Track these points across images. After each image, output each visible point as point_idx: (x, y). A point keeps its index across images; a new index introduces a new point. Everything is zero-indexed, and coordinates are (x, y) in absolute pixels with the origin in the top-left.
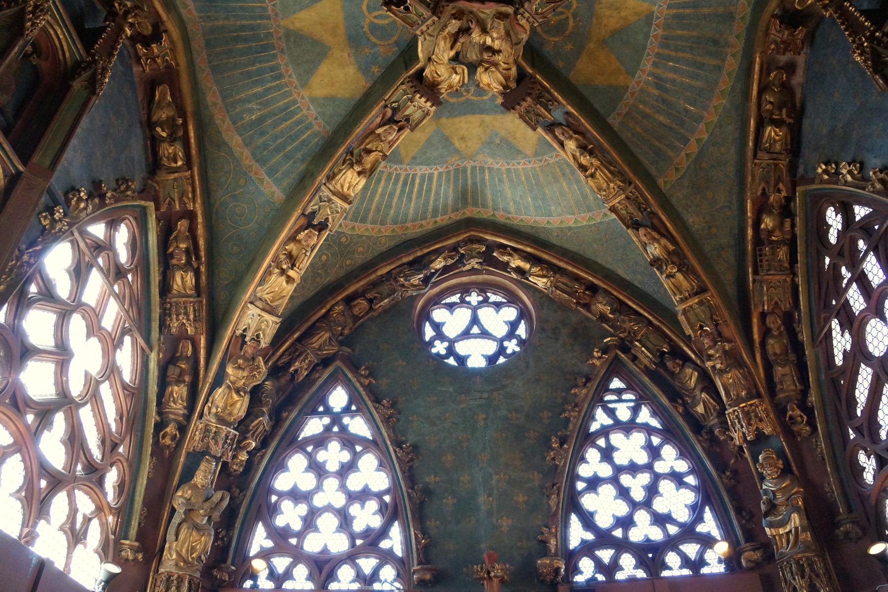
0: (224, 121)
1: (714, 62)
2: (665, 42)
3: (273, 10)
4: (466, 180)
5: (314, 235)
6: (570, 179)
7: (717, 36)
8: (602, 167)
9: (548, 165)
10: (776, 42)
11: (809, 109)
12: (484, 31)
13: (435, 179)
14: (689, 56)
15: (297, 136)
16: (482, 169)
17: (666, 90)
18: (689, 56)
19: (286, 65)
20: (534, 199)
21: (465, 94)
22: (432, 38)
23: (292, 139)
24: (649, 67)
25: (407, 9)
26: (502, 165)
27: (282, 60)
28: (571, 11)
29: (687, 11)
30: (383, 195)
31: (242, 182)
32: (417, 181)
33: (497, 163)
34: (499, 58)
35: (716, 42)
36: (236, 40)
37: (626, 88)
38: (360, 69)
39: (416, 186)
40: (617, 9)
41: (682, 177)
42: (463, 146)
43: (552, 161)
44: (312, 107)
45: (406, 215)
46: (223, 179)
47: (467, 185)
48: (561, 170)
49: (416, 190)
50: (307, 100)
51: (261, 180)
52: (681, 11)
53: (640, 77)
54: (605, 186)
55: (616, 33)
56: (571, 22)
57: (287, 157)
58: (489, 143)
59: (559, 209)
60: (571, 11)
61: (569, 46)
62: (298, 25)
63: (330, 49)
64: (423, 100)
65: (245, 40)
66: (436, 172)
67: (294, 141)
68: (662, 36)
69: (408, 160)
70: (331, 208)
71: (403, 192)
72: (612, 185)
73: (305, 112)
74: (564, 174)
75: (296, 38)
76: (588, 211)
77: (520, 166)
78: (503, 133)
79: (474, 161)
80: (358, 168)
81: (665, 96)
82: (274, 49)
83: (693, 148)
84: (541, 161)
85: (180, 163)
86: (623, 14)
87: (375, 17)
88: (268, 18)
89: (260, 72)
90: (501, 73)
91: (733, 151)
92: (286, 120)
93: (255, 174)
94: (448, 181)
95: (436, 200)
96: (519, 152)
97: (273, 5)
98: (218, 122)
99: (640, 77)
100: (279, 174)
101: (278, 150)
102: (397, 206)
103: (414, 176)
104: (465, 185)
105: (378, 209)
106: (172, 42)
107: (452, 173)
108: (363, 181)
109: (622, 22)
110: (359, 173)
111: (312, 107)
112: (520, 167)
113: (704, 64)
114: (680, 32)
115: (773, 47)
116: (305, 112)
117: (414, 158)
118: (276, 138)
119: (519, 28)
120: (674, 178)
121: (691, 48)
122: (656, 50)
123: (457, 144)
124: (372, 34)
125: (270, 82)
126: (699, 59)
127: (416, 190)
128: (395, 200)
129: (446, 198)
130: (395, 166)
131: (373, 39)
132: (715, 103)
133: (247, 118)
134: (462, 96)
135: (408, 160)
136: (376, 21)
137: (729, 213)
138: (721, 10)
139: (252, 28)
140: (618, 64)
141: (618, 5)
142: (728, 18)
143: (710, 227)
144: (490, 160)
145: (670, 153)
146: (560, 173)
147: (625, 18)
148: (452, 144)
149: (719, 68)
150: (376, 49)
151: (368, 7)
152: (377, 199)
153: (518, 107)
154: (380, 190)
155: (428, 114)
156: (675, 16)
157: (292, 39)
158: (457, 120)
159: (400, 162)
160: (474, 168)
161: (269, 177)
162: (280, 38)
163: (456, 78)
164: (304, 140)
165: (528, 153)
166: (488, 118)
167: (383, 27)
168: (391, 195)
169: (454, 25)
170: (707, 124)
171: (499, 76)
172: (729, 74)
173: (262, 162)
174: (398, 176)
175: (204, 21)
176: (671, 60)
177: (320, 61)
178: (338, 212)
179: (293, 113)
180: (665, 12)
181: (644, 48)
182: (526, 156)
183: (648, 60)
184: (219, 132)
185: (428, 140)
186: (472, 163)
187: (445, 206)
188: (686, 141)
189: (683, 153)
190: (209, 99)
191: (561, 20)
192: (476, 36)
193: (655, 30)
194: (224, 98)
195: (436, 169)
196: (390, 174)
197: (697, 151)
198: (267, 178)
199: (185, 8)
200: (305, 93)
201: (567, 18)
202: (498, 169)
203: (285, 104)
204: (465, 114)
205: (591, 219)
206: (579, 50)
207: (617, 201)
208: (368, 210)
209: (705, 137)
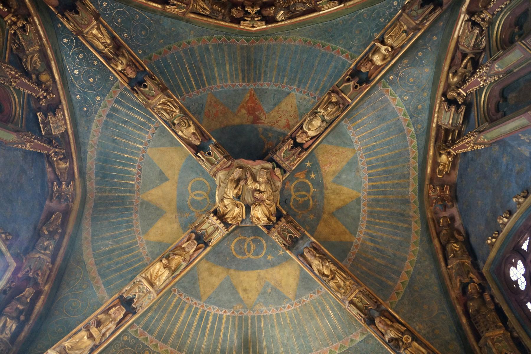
0: (87, 249)
1: (405, 225)
2: (371, 214)
3: (138, 187)
4: (248, 329)
5: (122, 310)
6: (322, 315)
7: (402, 212)
8: (339, 271)
9: (305, 305)
10: (435, 199)
11: (470, 229)
12: (255, 180)
13: (224, 321)
14: (388, 222)
15: (131, 265)
16: (259, 317)
17: (378, 243)
18: (388, 222)
19: (137, 220)
20: (298, 338)
21: (247, 253)
22: (224, 185)
23: (128, 265)
24: (364, 229)
25: (209, 154)
26: (273, 311)
27: (135, 217)
28: (311, 194)
29: (380, 197)
30: (183, 323)
31: (84, 286)
32: (211, 319)
33: (269, 310)
34: (265, 196)
35: (402, 215)
36: (112, 204)
37: (351, 243)
38: (181, 225)
39: (210, 323)
40: (337, 194)
41: (403, 298)
42: (246, 296)
43: (308, 301)
44: (146, 248)
45: (199, 348)
46: (72, 282)
47: (248, 332)
48: (315, 308)
49: (209, 326)
50: (144, 242)
51: (98, 288)
52: (376, 197)
53: (359, 235)
54: (342, 284)
55: (339, 209)
56: (311, 202)
57: (121, 276)
58: (263, 293)
59: (317, 344)
60: (311, 194)
61: (312, 217)
62: (150, 198)
63: (165, 212)
64: (215, 218)
65: (117, 205)
66: (225, 315)
67: (129, 267)
68: (368, 211)
69: (205, 298)
70: (139, 288)
71: (199, 325)
72: (348, 283)
73: (141, 250)
74: (317, 311)
75: (146, 205)
76: (339, 340)
77: (288, 309)
78: (272, 283)
79: (254, 311)
80: (165, 262)
81: (378, 246)
82: (133, 210)
83: (405, 278)
84: (300, 302)
85: (48, 252)
86: (342, 198)
87: (195, 195)
88: (134, 192)
89: (119, 223)
90: (265, 206)
91: (433, 276)
92: (127, 254)
93: (96, 283)
94: (234, 325)
95: (224, 341)
96: (285, 297)
97: (138, 183)
98: (84, 248)
99: (359, 235)
100: (112, 286)
101: (116, 271)
102: (193, 338)
103: (209, 313)
104: (247, 334)
105: (178, 336)
106: (75, 190)
107: (237, 319)
108: (167, 273)
109: (342, 202)
110: (165, 267)
111: (146, 248)
112: (285, 311)
113: (398, 226)
114: (378, 209)
115: (434, 201)
116: (141, 250)
117: (210, 298)
118: (117, 263)
119: (276, 178)
120: (397, 300)
121: (388, 218)
122: (366, 219)
123: (242, 294)
124: (192, 205)
125: (125, 229)
126: (394, 223)
127: (209, 326)
128: (192, 331)
129: (232, 342)
130: (195, 301)
131: (192, 209)
132: (412, 249)
133: (103, 249)
134: (245, 255)
135: (205, 298)
136: (195, 198)
137: (444, 317)
138: (400, 197)
139: (123, 198)
140: (344, 227)
141: (338, 191)
142: (406, 202)
143: (433, 330)
144: (264, 309)
145: (390, 283)
146: (315, 312)
147: (344, 200)
148: (237, 293)
149: (409, 229)
150: (193, 214)
151: (191, 189)
152: (179, 324)
153: (276, 226)
154: (182, 318)
155: (217, 229)
156: (373, 200)
157: (144, 206)
158: (242, 273)
159: (199, 298)
160: (253, 317)
161: (104, 286)
162: (137, 205)
163: (237, 210)
164: (135, 268)
165: (290, 296)
166: (262, 272)
167: (198, 202)
168: (190, 325)
169: (237, 173)
170: (410, 262)
171: (264, 208)
172: (416, 232)
173: (103, 276)
174: (197, 309)
175: (98, 192)
176: (377, 225)
177: (157, 220)
178: (143, 292)
179: (133, 250)
180: (367, 197)
181: (359, 218)
182: (289, 300)
183: (363, 225)
184: (82, 254)
185: (221, 285)
186: (252, 314)
187: (231, 348)
188: (399, 273)
189: (399, 282)
190: (84, 235)
191: (305, 201)
192: (251, 185)
193: (364, 208)
194: (93, 236)
195: (225, 312)
196: (191, 307)
197: (408, 279)
198: (103, 287)
199: (90, 181)
200: (144, 238)
201: (309, 199)
202: (271, 315)
203: (130, 243)
204: (246, 270)
205: (342, 347)
206: (318, 218)
207: (353, 295)
208: (170, 333)
209: (411, 269)
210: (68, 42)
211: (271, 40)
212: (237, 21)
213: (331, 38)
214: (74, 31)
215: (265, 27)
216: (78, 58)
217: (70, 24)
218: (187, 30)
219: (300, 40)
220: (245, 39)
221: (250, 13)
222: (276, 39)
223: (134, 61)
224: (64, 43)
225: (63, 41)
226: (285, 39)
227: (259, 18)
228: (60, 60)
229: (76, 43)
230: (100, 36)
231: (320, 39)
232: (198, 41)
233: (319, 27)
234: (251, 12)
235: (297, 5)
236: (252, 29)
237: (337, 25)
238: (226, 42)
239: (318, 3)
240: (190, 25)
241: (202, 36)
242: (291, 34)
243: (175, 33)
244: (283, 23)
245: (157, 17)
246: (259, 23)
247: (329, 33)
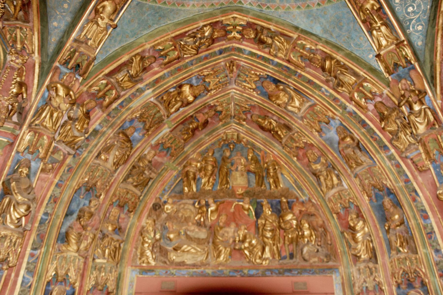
210: (418, 26)
211: (217, 4)
212: (250, 25)
213: (158, 11)
214: (404, 46)
215: (223, 18)
216: (414, 8)
217: (406, 54)
218: (299, 20)
219: (188, 5)
220: (243, 4)
221: (237, 32)
222: (213, 5)
223: (355, 6)
224: (422, 25)
225: (423, 28)
226: (203, 5)
227: (228, 28)
228: (434, 7)
229: (410, 24)
230: (381, 39)
231: (168, 9)
232: (289, 8)
233: (170, 20)
234: (236, 34)
235: (192, 43)
236: (235, 15)
237: (154, 24)
238: (261, 4)
239: (173, 47)
240: (295, 23)
241: (285, 13)
242: (197, 11)
243: (311, 18)
244: (205, 23)
245: (325, 36)
246: (228, 22)
247: (160, 16)
